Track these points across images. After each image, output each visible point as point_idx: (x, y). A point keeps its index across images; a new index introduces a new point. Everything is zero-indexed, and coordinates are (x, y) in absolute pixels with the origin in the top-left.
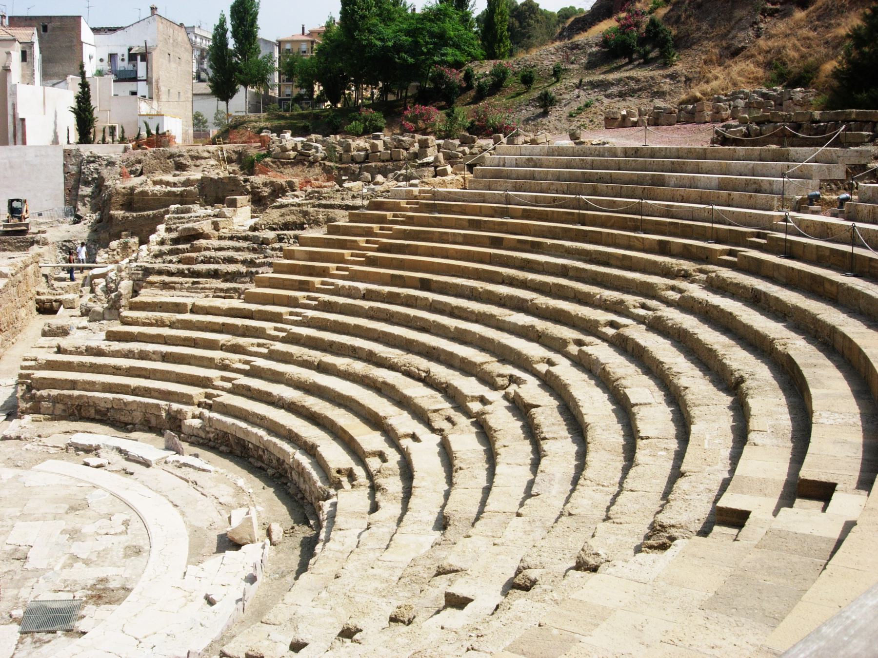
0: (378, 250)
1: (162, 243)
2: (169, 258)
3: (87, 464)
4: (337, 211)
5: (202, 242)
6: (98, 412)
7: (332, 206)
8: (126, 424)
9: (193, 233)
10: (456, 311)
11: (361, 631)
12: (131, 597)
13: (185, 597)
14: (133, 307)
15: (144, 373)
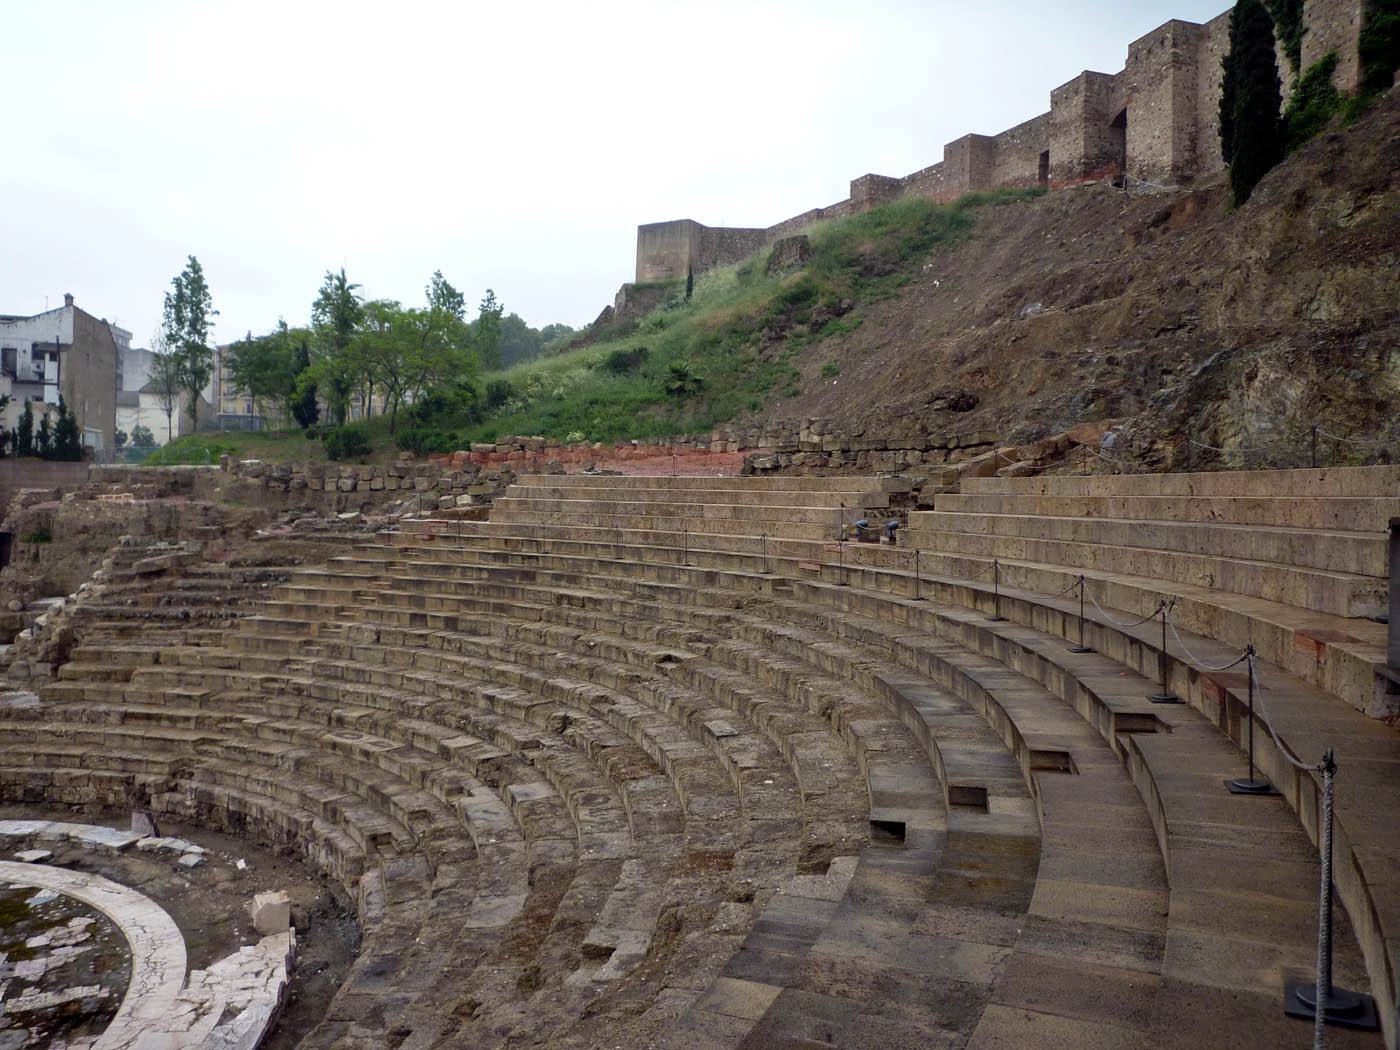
0: (392, 587)
1: (111, 581)
2: (124, 598)
3: (20, 860)
4: (334, 545)
5: (166, 580)
6: (27, 792)
7: (327, 539)
8: (70, 805)
9: (154, 569)
10: (492, 653)
11: (480, 1004)
12: (117, 1023)
13: (195, 1010)
14: (81, 658)
15: (97, 739)
